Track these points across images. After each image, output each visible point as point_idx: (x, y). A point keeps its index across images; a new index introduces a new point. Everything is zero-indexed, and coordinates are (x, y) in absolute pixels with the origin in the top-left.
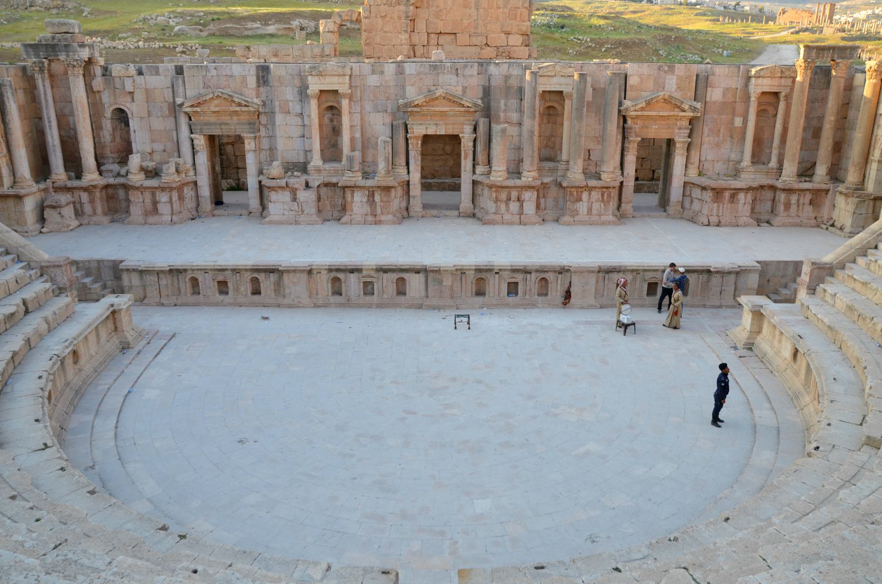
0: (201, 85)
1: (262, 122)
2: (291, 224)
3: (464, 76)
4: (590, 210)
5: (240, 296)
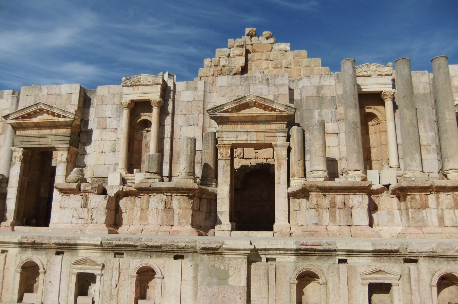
3: (275, 85)
4: (441, 219)
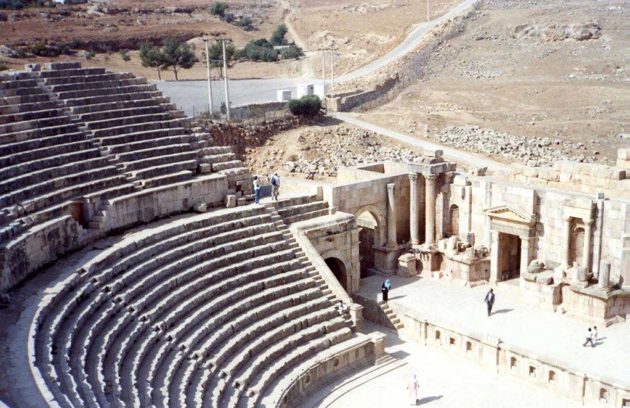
1: (538, 229)
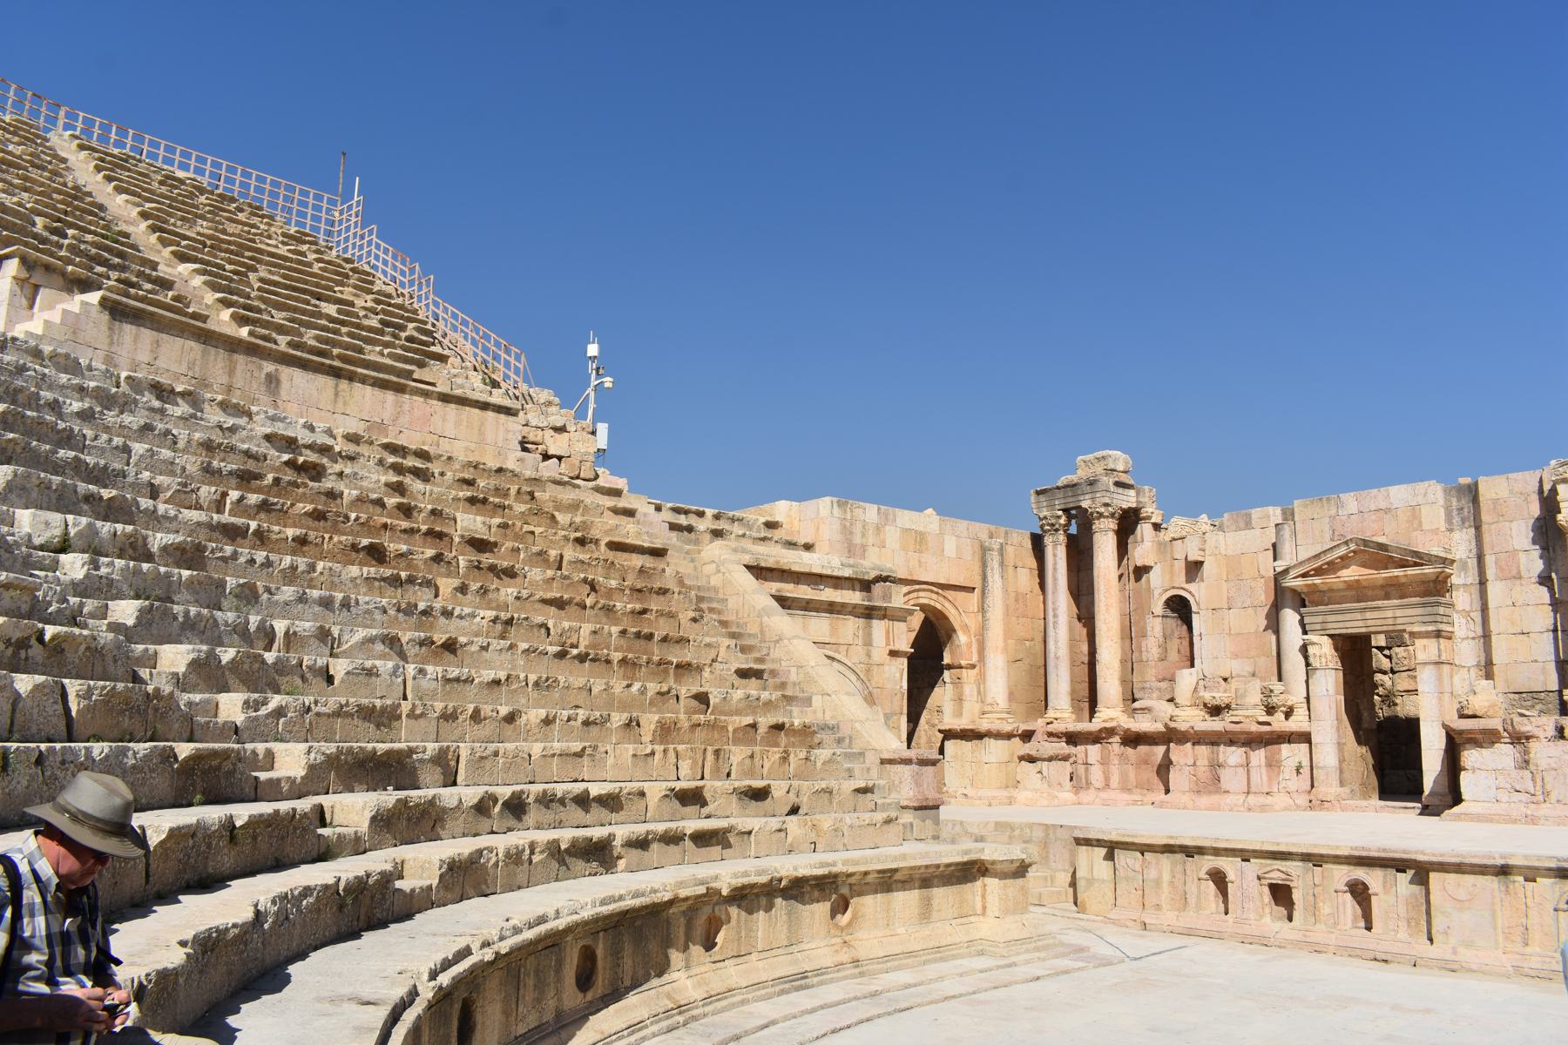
0: (1328, 536)
2: (1515, 821)
5: (1320, 927)
